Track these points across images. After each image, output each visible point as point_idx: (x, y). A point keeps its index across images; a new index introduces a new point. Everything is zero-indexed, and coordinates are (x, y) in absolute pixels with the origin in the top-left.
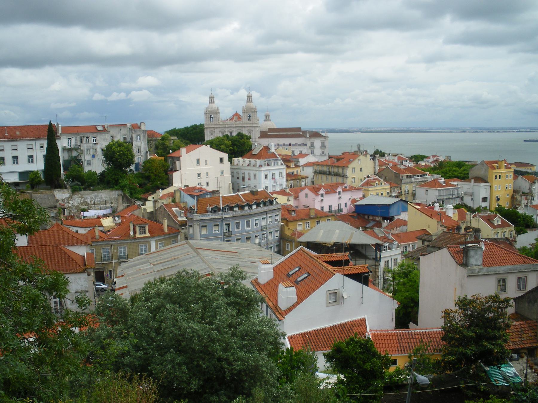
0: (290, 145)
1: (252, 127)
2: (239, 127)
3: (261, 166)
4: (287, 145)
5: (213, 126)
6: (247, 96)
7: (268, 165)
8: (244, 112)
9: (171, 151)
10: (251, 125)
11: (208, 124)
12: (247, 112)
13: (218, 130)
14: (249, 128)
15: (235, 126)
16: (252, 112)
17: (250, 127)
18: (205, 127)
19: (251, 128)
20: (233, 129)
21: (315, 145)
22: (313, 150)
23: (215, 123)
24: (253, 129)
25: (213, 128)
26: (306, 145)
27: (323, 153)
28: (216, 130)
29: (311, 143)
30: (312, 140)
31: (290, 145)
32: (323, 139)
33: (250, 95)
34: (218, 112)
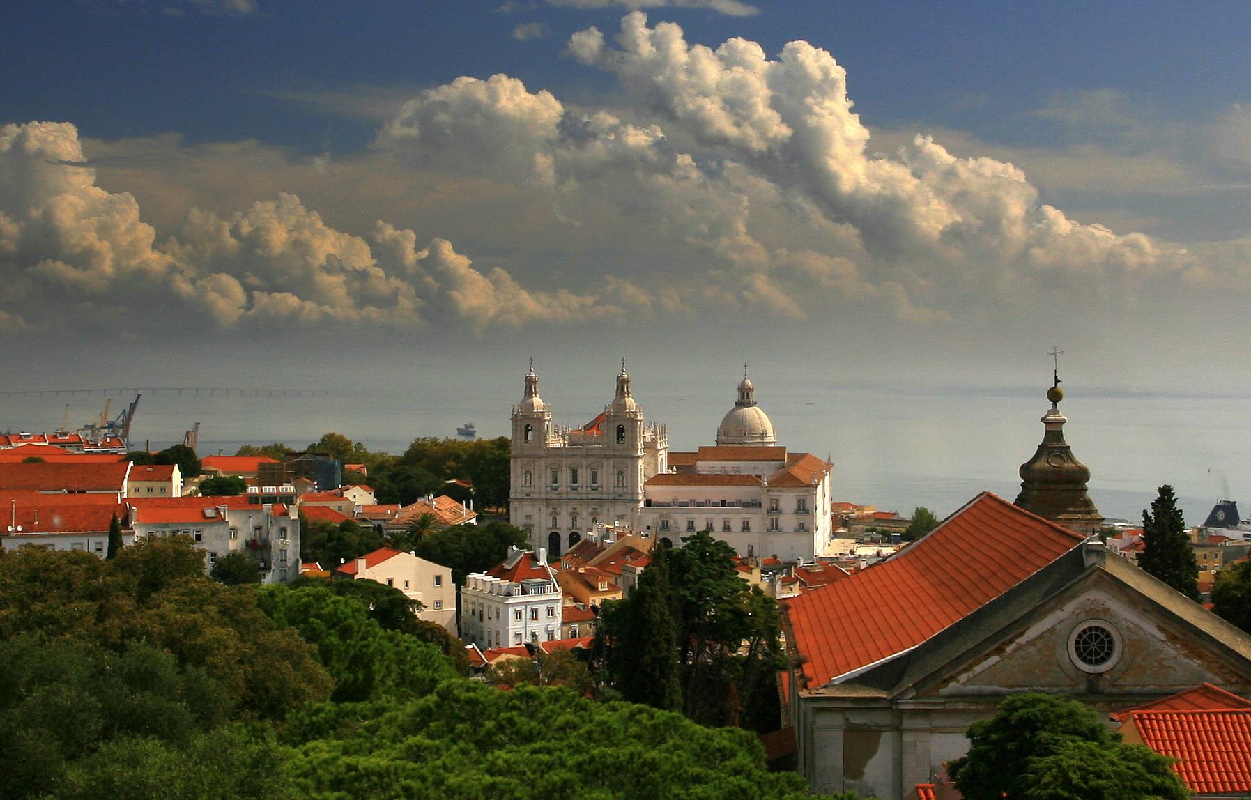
3: (509, 594)
4: (715, 504)
7: (524, 592)
9: (342, 561)
10: (623, 453)
17: (621, 456)
18: (512, 453)
32: (801, 493)
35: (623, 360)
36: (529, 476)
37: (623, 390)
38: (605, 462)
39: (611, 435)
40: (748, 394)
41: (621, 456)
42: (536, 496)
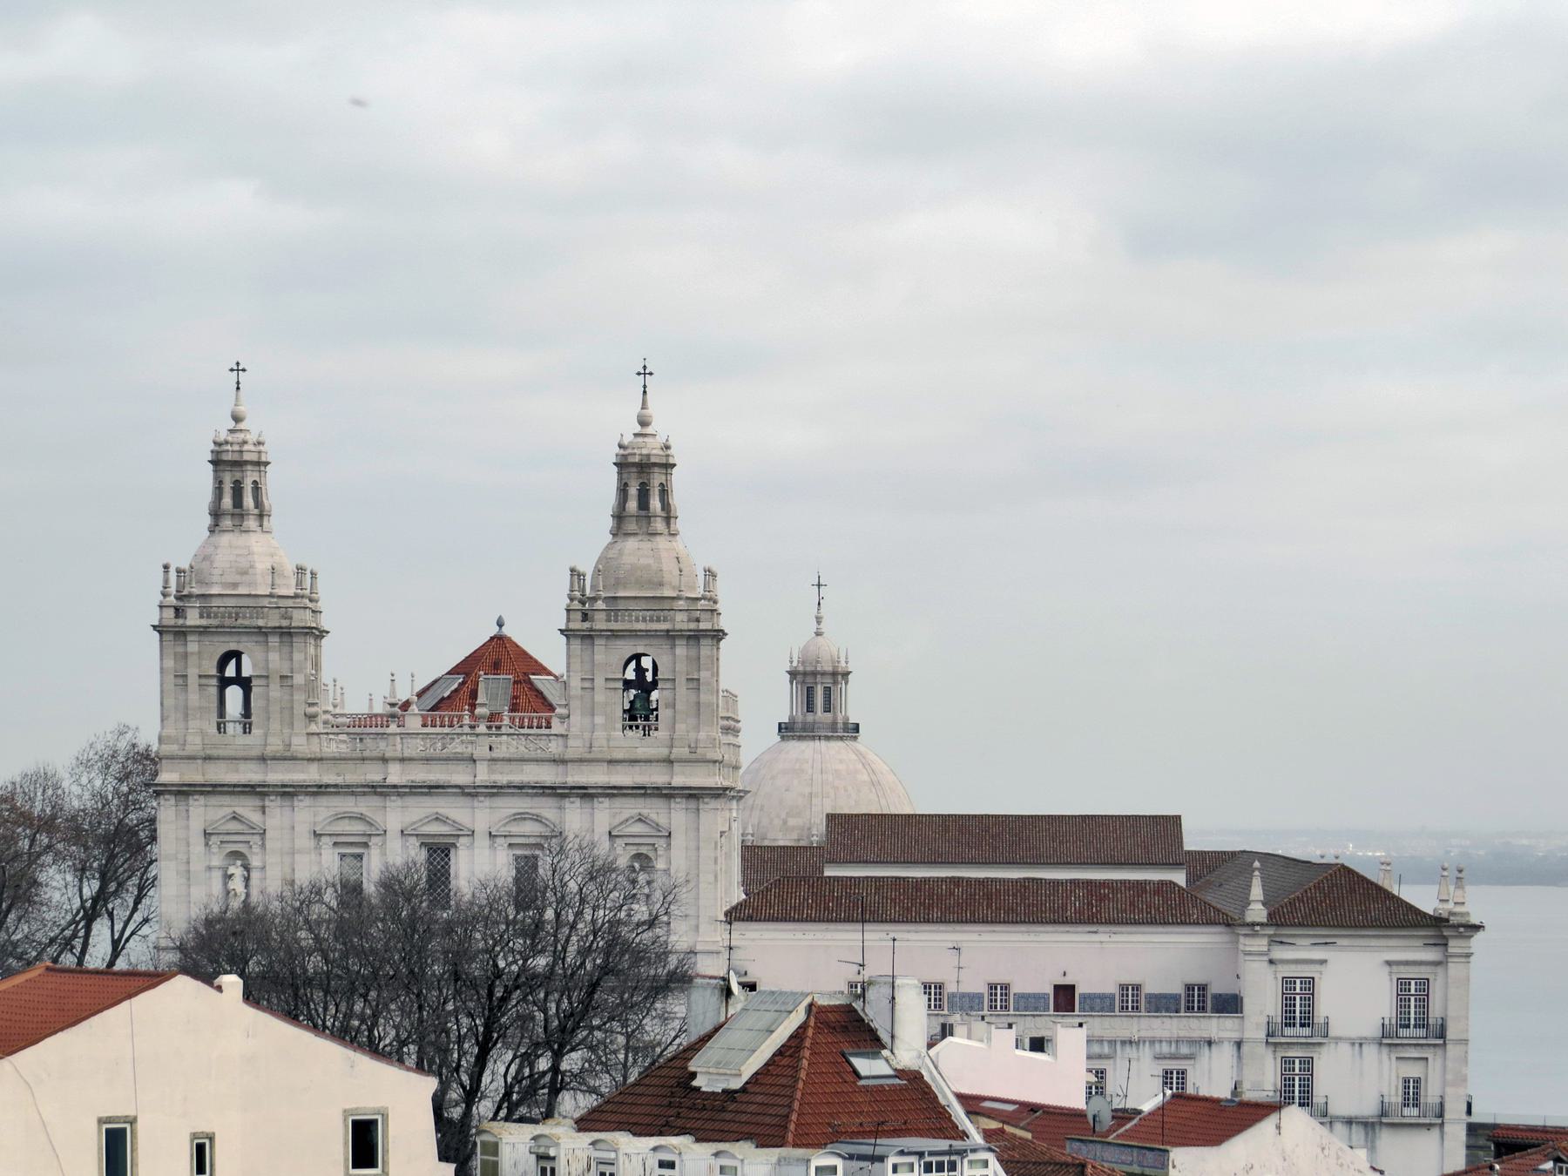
1: (666, 794)
2: (520, 789)
5: (250, 774)
6: (622, 465)
8: (588, 637)
10: (657, 777)
11: (195, 744)
12: (614, 635)
13: (308, 814)
14: (631, 807)
15: (483, 775)
16: (670, 636)
17: (642, 791)
19: (654, 810)
20: (458, 811)
21: (1325, 1007)
22: (1308, 1063)
23: (275, 746)
24: (676, 816)
25: (250, 790)
26: (1230, 1004)
27: (1412, 1091)
28: (277, 817)
29: (1288, 982)
30: (1301, 950)
31: (1065, 997)
33: (652, 448)
34: (301, 618)
35: (645, 372)
36: (237, 871)
37: (644, 503)
39: (600, 697)
40: (828, 692)
41: (642, 791)
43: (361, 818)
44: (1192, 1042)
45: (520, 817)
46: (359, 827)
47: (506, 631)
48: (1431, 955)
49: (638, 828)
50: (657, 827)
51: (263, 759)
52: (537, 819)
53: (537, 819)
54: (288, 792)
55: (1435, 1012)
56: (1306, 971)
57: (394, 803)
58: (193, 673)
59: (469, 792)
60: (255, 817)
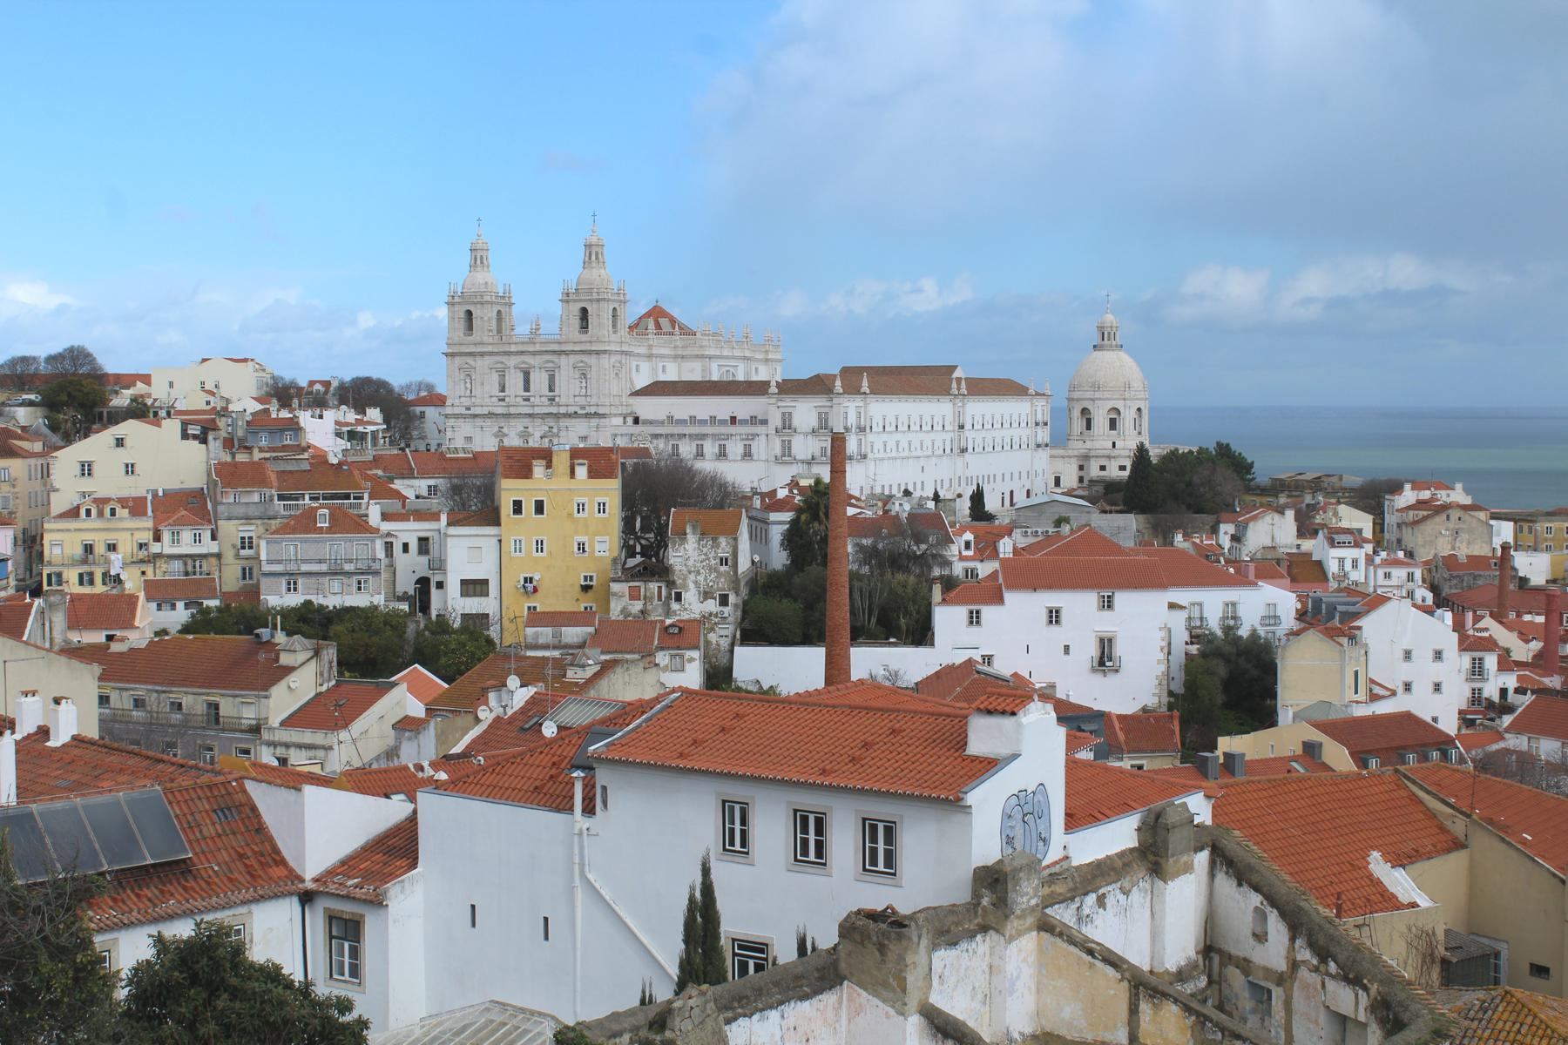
0: (733, 420)
4: (723, 422)
5: (472, 349)
8: (567, 302)
12: (575, 301)
13: (489, 360)
16: (591, 301)
20: (530, 360)
21: (796, 422)
22: (789, 441)
23: (479, 340)
24: (592, 360)
25: (471, 354)
26: (764, 422)
29: (784, 414)
30: (787, 402)
31: (733, 420)
33: (594, 240)
35: (594, 215)
36: (468, 381)
38: (563, 360)
42: (478, 411)
43: (502, 363)
44: (752, 435)
45: (548, 361)
46: (502, 366)
47: (659, 304)
48: (829, 404)
49: (581, 365)
50: (586, 363)
51: (475, 344)
52: (553, 362)
53: (553, 362)
54: (482, 354)
55: (830, 424)
56: (789, 410)
57: (513, 357)
58: (456, 317)
59: (534, 353)
60: (472, 363)
